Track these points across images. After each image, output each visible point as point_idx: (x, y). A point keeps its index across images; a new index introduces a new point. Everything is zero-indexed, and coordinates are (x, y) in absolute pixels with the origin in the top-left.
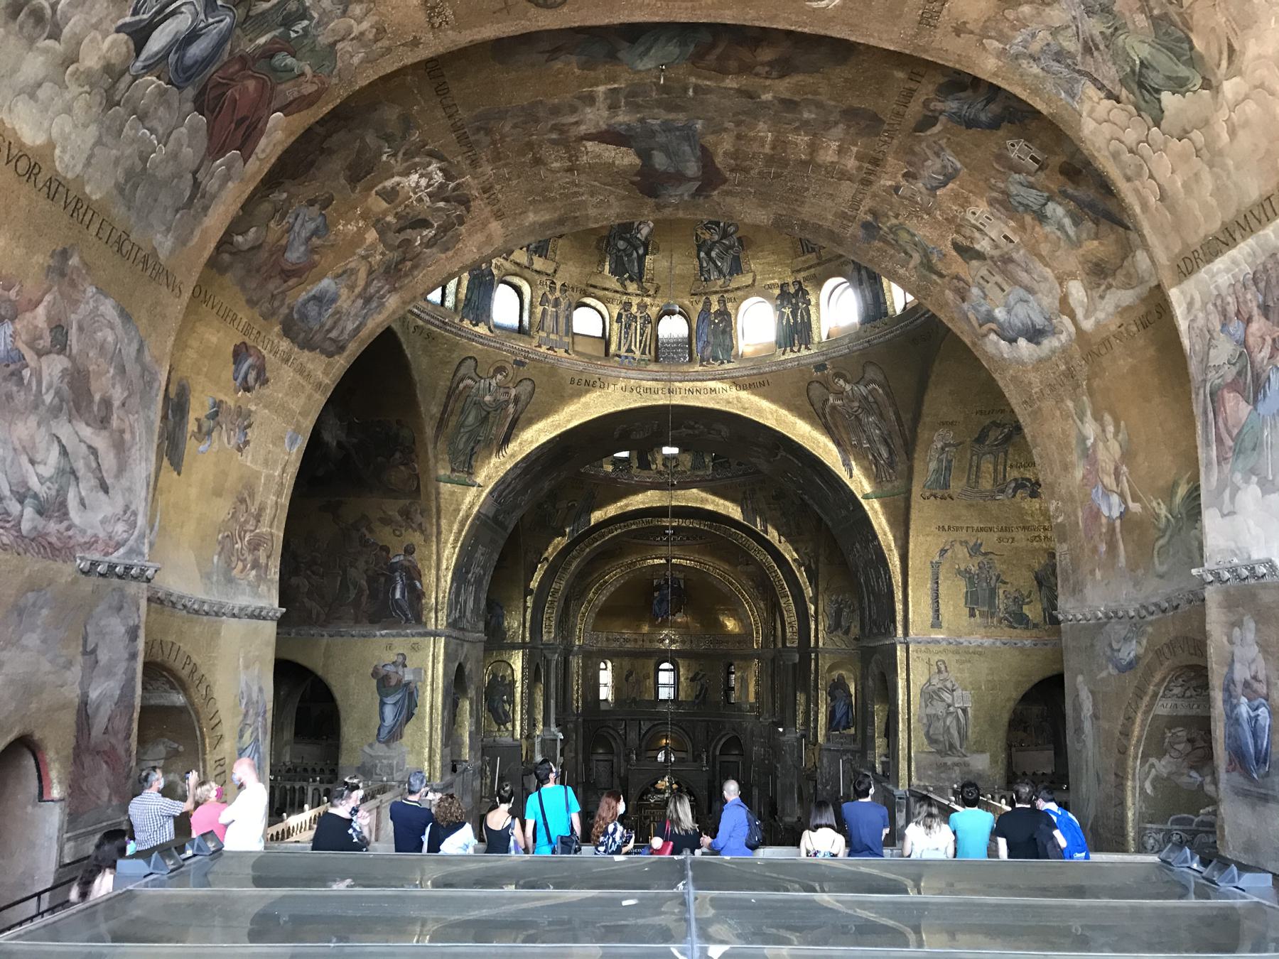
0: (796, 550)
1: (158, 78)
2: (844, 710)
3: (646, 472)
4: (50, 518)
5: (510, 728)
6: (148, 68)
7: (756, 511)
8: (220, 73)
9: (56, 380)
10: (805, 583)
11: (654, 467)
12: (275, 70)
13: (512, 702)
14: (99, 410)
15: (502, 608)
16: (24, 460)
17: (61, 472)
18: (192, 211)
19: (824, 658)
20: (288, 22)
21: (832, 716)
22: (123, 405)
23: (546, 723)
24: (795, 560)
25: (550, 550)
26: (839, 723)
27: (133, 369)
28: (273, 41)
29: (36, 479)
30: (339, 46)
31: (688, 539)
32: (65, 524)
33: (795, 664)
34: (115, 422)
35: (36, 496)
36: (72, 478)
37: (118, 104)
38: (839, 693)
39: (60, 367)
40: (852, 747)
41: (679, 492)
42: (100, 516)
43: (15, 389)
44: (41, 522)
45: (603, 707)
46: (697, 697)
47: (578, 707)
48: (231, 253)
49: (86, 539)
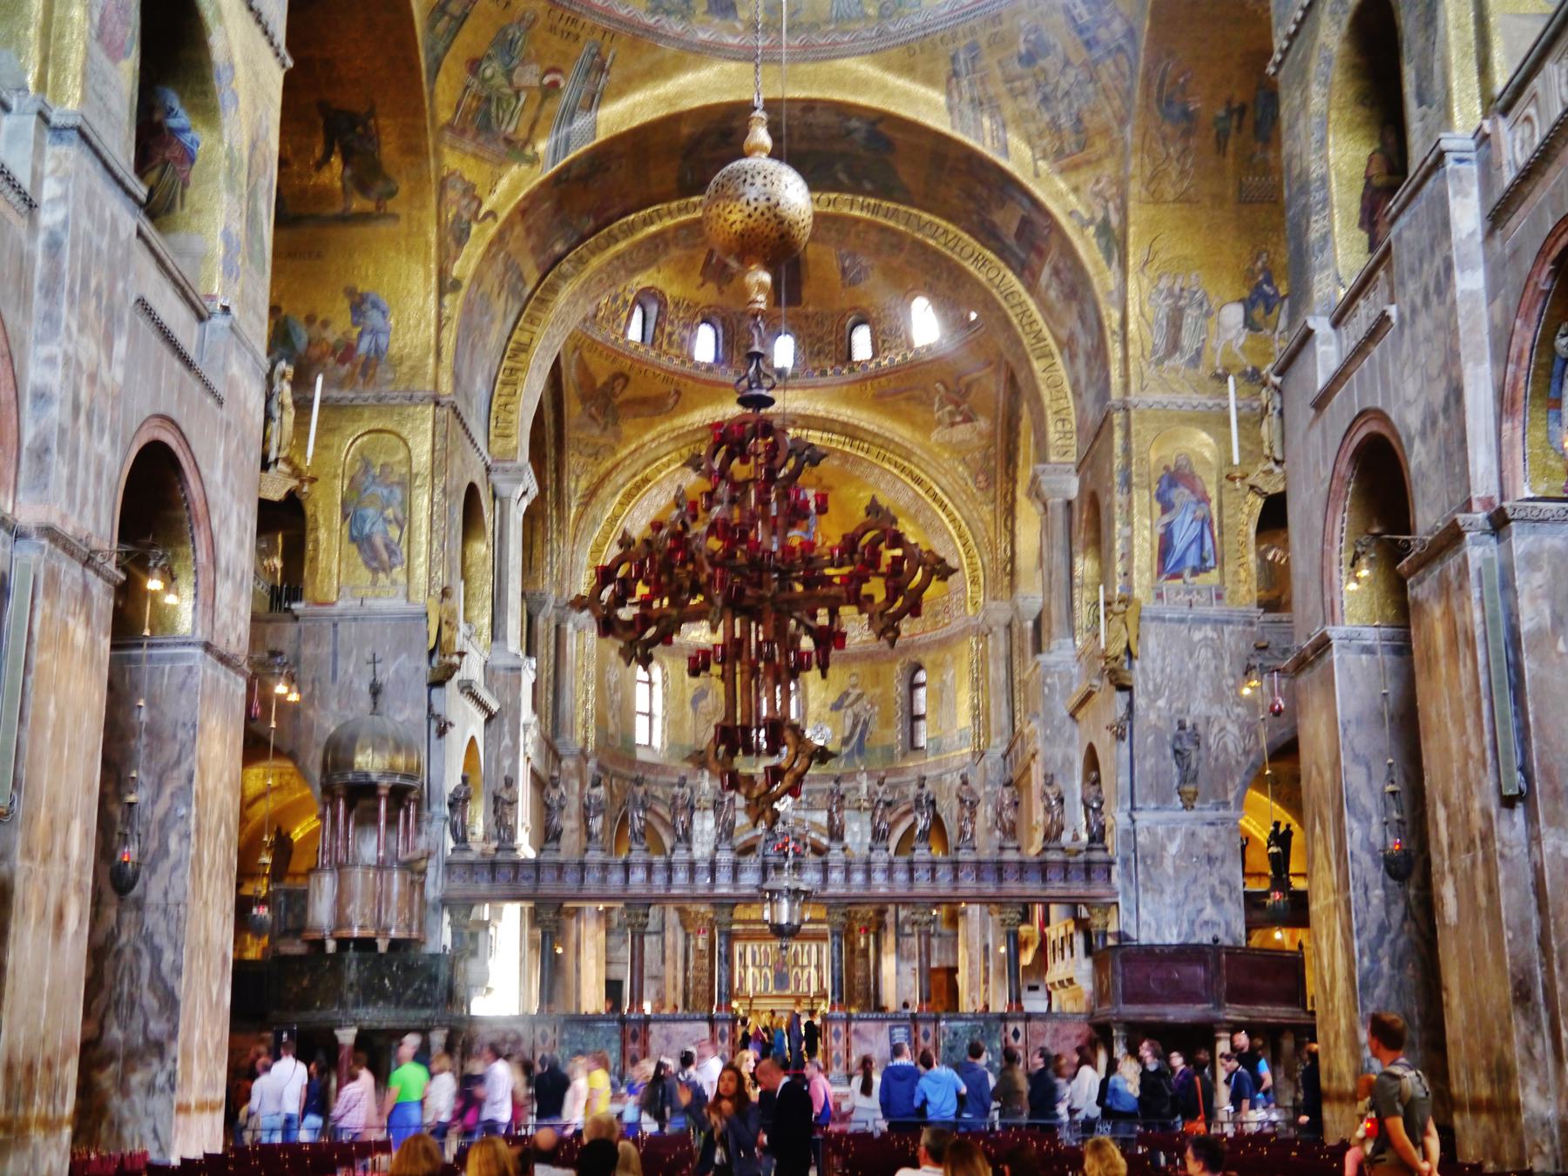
0: (1076, 190)
2: (1194, 530)
3: (728, 22)
5: (402, 579)
7: (978, 104)
10: (1096, 264)
11: (743, 14)
13: (404, 522)
15: (384, 314)
19: (1142, 418)
21: (1165, 546)
23: (497, 631)
24: (1071, 214)
25: (503, 184)
26: (1181, 561)
31: (824, 373)
33: (1069, 504)
38: (1180, 495)
40: (1213, 610)
41: (802, 67)
45: (642, 755)
46: (845, 742)
47: (586, 740)
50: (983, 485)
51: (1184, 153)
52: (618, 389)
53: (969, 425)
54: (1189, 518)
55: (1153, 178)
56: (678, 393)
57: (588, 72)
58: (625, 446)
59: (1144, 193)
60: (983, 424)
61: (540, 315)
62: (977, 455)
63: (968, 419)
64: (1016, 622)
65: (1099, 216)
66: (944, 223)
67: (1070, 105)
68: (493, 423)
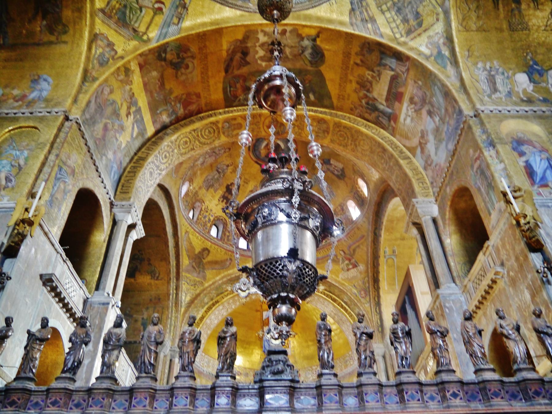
2: (545, 164)
50: (364, 295)
51: (478, 7)
52: (205, 256)
53: (355, 269)
54: (538, 159)
55: (464, 19)
56: (231, 259)
57: (177, 7)
58: (207, 282)
59: (460, 27)
60: (362, 267)
61: (153, 147)
62: (360, 283)
63: (355, 266)
64: (387, 352)
65: (435, 52)
66: (348, 115)
67: (412, 7)
68: (120, 187)
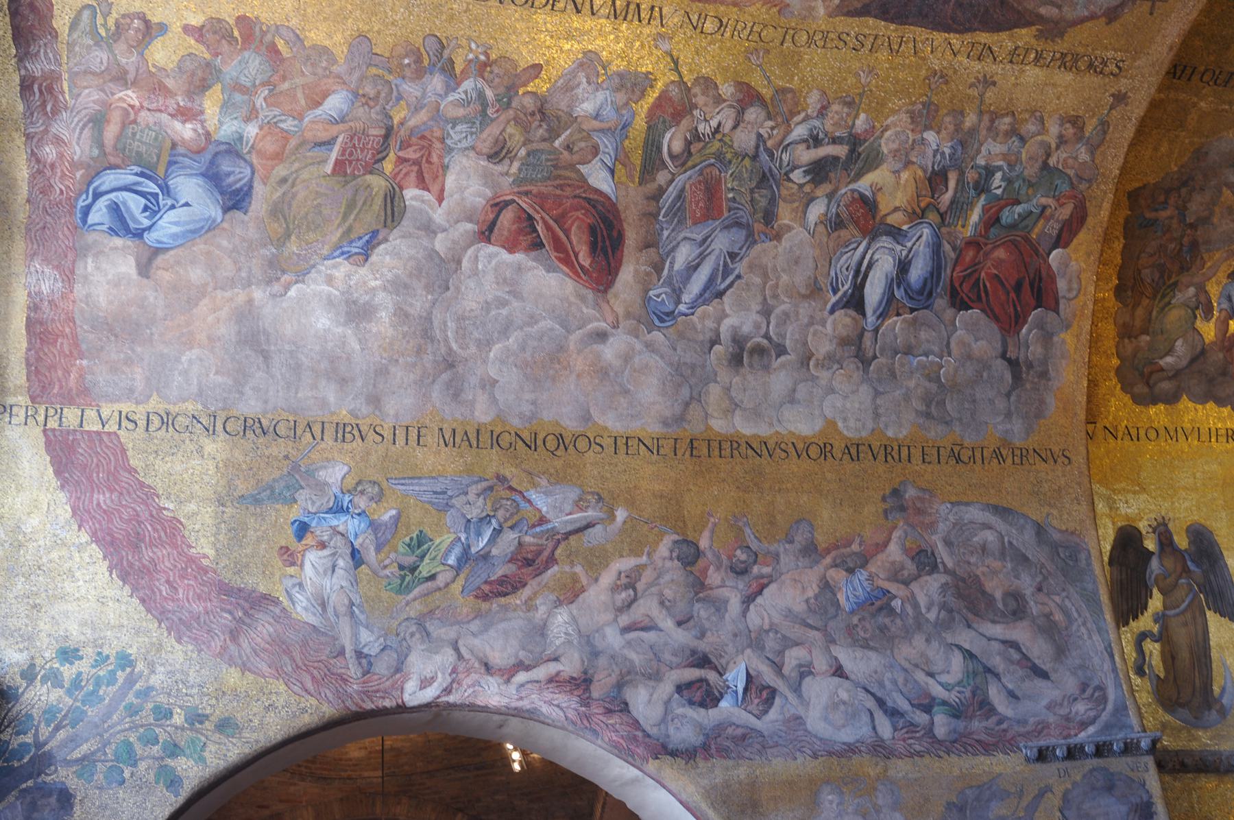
1: (898, 314)
4: (971, 718)
6: (883, 316)
8: (958, 269)
9: (936, 598)
12: (1013, 226)
14: (1005, 605)
16: (920, 676)
17: (971, 674)
18: (1028, 386)
20: (982, 187)
22: (1040, 589)
27: (1037, 554)
28: (985, 210)
29: (940, 688)
30: (1052, 162)
32: (994, 719)
34: (1034, 609)
35: (944, 703)
36: (989, 676)
37: (875, 357)
39: (936, 585)
42: (1044, 702)
43: (887, 621)
44: (961, 725)
48: (1170, 378)
49: (1029, 728)
